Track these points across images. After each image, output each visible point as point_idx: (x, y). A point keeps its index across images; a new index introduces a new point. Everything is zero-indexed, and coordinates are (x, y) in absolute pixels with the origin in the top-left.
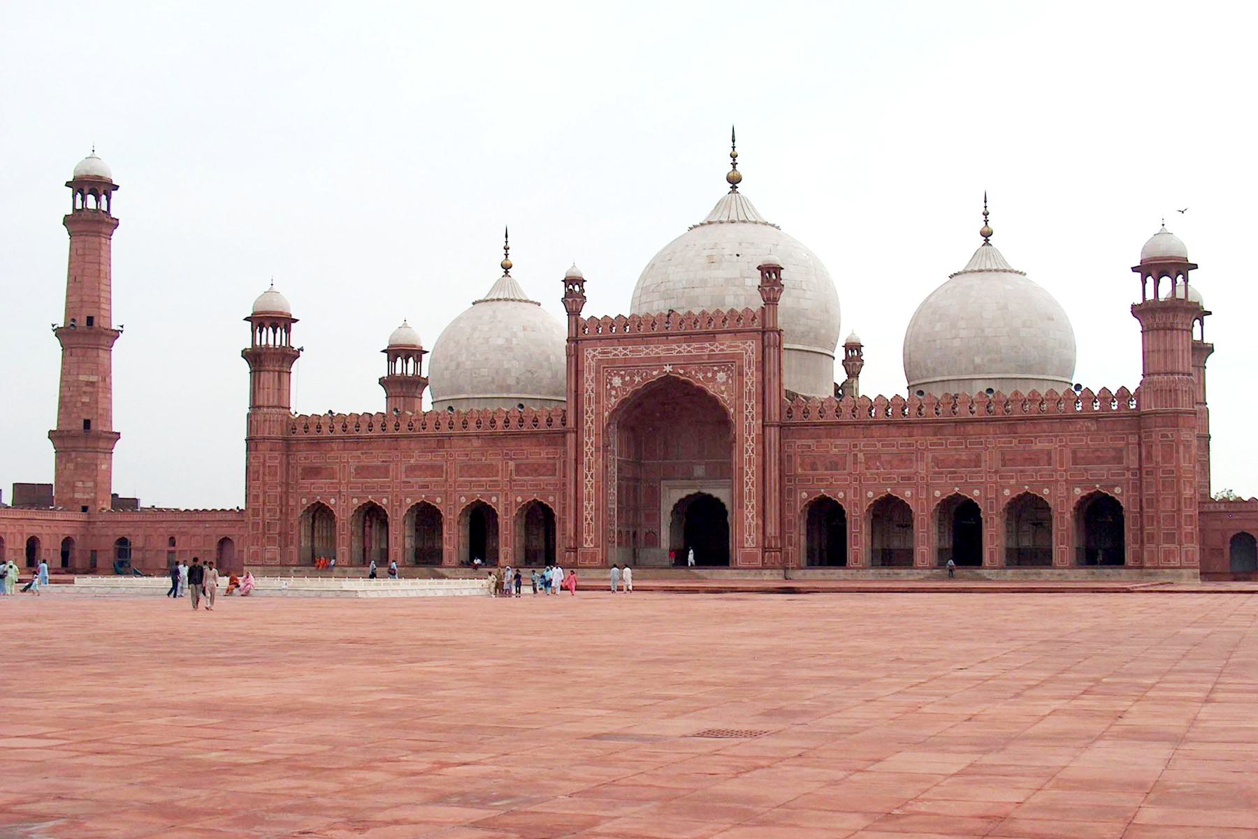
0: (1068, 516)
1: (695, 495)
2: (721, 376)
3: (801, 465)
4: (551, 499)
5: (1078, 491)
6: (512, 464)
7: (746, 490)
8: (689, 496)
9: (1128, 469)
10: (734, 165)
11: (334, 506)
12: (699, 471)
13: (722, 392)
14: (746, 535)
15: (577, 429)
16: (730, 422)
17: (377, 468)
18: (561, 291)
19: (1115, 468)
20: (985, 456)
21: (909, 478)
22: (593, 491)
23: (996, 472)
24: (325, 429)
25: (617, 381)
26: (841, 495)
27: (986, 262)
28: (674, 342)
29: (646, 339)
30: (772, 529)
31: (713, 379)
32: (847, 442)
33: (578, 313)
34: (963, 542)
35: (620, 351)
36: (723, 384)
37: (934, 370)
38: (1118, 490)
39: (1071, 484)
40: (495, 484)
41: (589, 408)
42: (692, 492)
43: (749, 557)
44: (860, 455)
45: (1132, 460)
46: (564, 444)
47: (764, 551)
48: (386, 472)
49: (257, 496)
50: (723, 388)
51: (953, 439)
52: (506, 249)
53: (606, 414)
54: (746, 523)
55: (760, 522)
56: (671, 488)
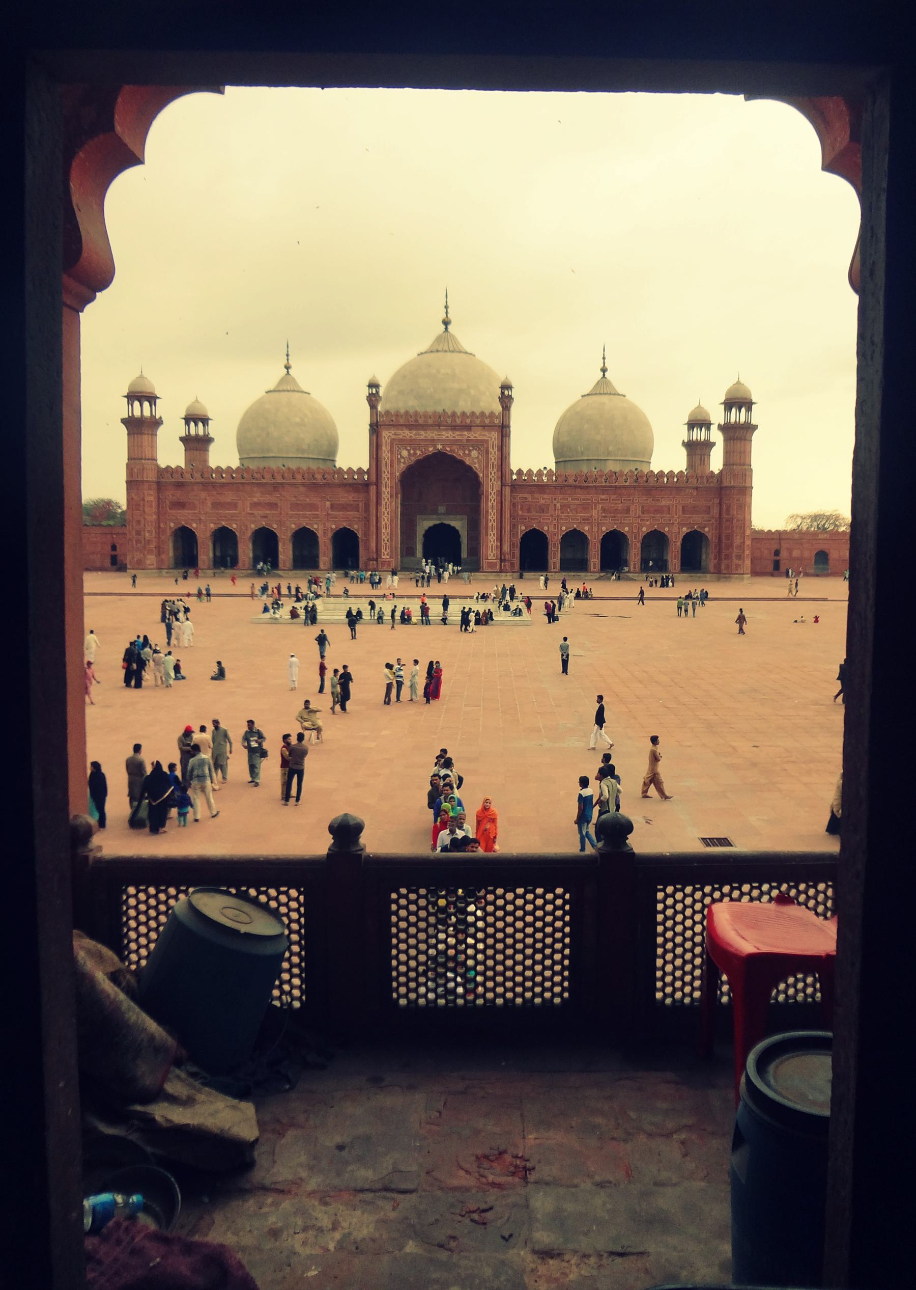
0: (679, 544)
2: (474, 453)
3: (521, 509)
5: (685, 530)
6: (328, 504)
7: (490, 524)
8: (435, 526)
9: (713, 518)
11: (196, 529)
12: (442, 509)
14: (489, 552)
15: (378, 483)
17: (228, 503)
18: (366, 391)
19: (706, 517)
20: (633, 508)
22: (388, 523)
23: (639, 517)
24: (188, 476)
25: (405, 453)
26: (546, 528)
27: (603, 387)
29: (425, 427)
30: (506, 548)
31: (469, 455)
32: (549, 496)
34: (613, 556)
37: (582, 453)
38: (707, 529)
39: (681, 525)
40: (316, 516)
43: (491, 565)
44: (558, 505)
45: (715, 511)
46: (367, 492)
47: (501, 562)
48: (234, 506)
49: (139, 522)
51: (614, 497)
53: (398, 474)
54: (490, 545)
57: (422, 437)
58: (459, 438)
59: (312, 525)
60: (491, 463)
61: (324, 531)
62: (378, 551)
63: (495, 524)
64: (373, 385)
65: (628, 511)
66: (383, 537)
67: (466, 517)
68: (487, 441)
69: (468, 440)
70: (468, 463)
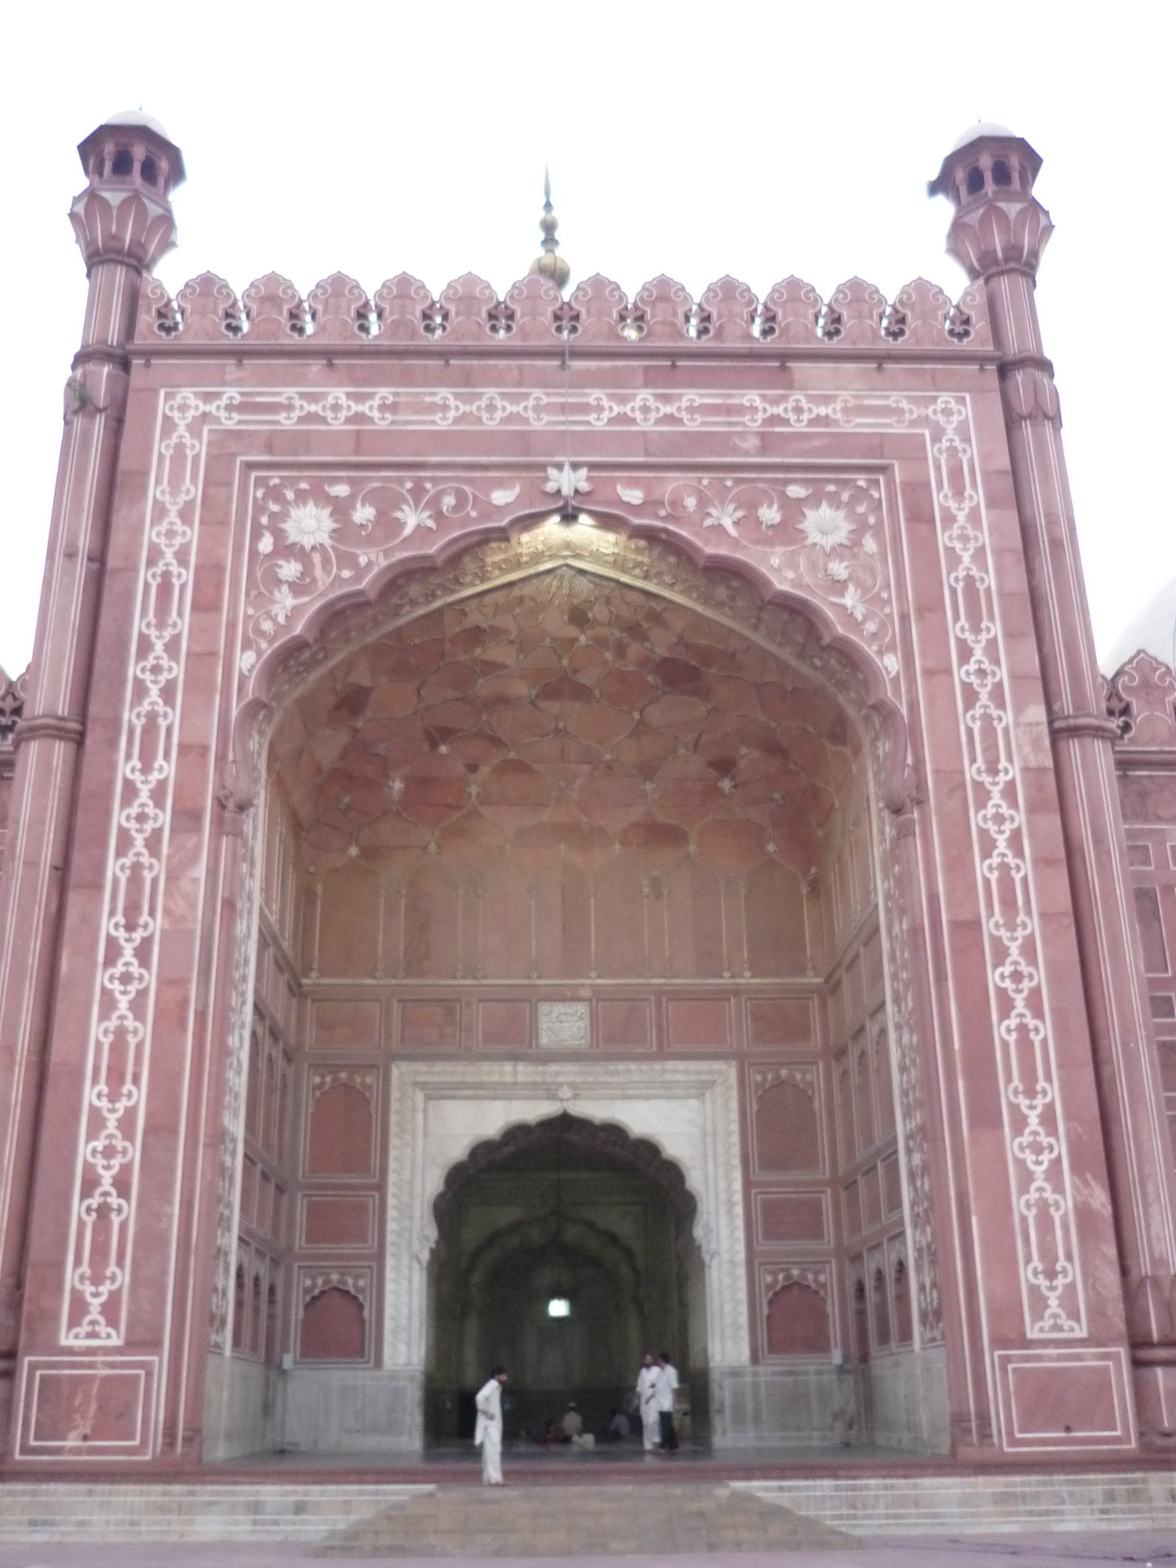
1: (547, 1125)
2: (825, 524)
7: (1003, 1031)
8: (516, 1132)
10: (550, 241)
12: (563, 1024)
13: (839, 587)
14: (1029, 1274)
15: (82, 729)
16: (884, 712)
22: (142, 1033)
25: (310, 524)
31: (788, 531)
33: (137, 262)
35: (335, 404)
36: (838, 552)
42: (534, 1111)
43: (1048, 1398)
47: (1137, 1363)
50: (839, 569)
53: (246, 661)
54: (1022, 1206)
55: (1100, 1199)
56: (436, 1093)
57: (442, 422)
58: (716, 424)
60: (952, 580)
63: (1044, 1031)
64: (131, 160)
66: (85, 1150)
67: (729, 1072)
70: (781, 585)
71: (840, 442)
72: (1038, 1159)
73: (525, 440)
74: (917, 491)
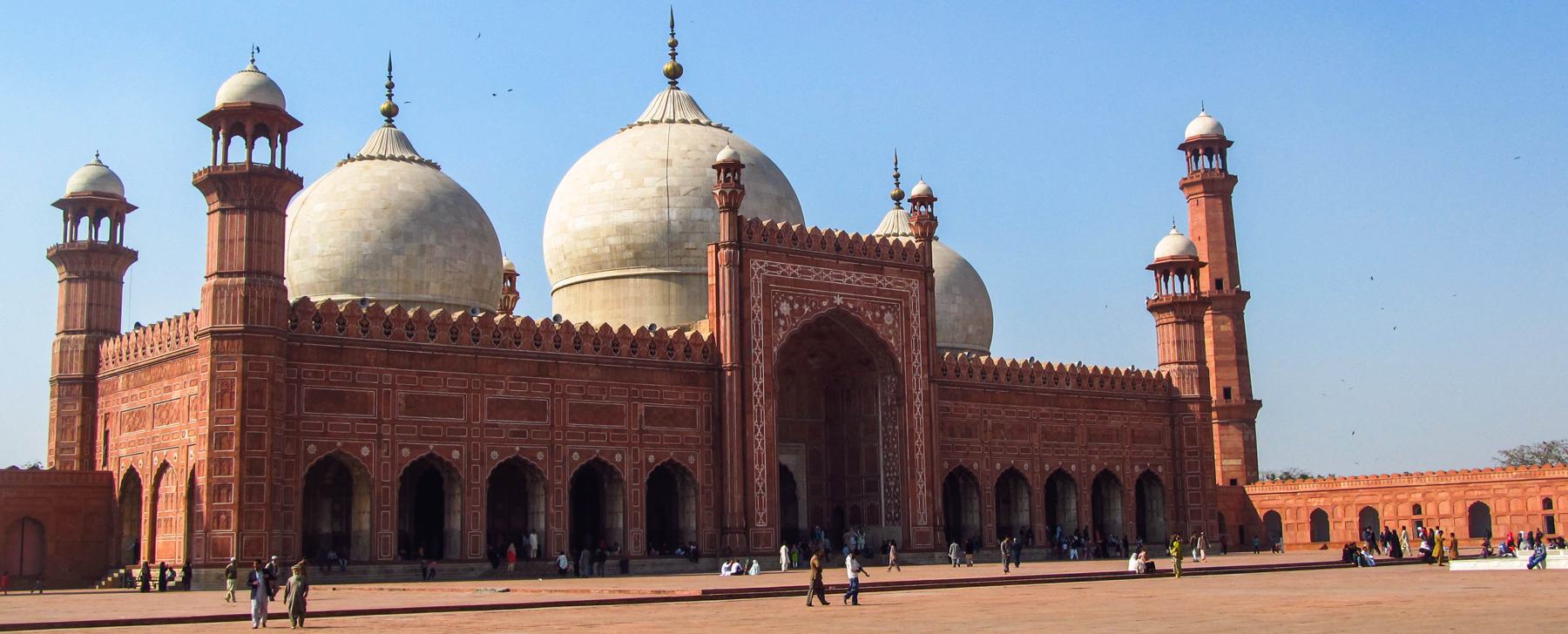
2: (888, 318)
4: (691, 460)
6: (642, 406)
10: (673, 55)
21: (1026, 450)
25: (785, 308)
26: (976, 466)
28: (846, 268)
38: (1160, 469)
41: (758, 338)
43: (922, 537)
45: (1167, 443)
48: (455, 406)
49: (257, 440)
51: (1056, 410)
52: (390, 86)
59: (613, 455)
61: (631, 470)
62: (747, 511)
65: (1071, 436)
68: (905, 296)
69: (880, 293)
71: (893, 294)
72: (921, 484)
73: (829, 287)
74: (907, 309)
